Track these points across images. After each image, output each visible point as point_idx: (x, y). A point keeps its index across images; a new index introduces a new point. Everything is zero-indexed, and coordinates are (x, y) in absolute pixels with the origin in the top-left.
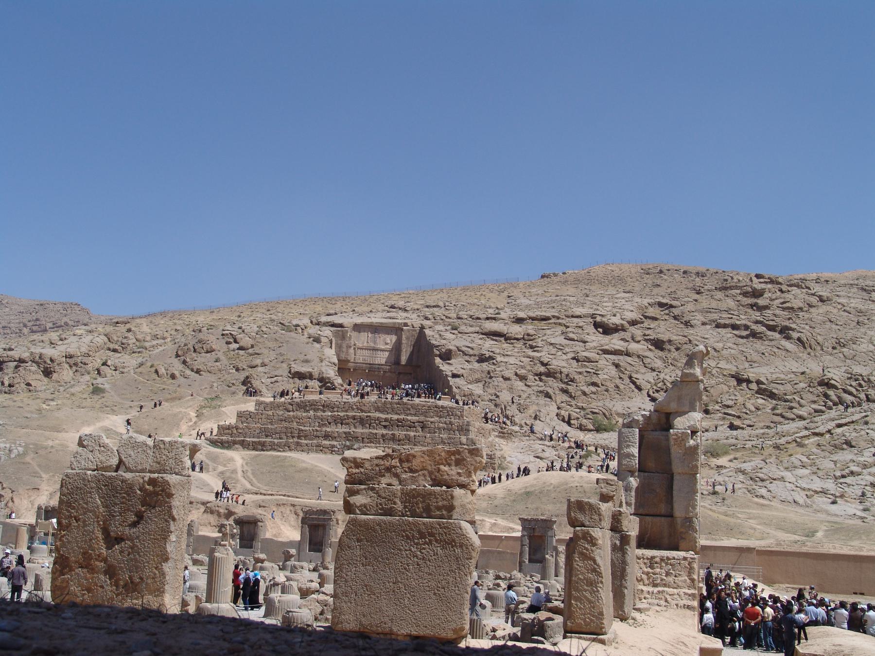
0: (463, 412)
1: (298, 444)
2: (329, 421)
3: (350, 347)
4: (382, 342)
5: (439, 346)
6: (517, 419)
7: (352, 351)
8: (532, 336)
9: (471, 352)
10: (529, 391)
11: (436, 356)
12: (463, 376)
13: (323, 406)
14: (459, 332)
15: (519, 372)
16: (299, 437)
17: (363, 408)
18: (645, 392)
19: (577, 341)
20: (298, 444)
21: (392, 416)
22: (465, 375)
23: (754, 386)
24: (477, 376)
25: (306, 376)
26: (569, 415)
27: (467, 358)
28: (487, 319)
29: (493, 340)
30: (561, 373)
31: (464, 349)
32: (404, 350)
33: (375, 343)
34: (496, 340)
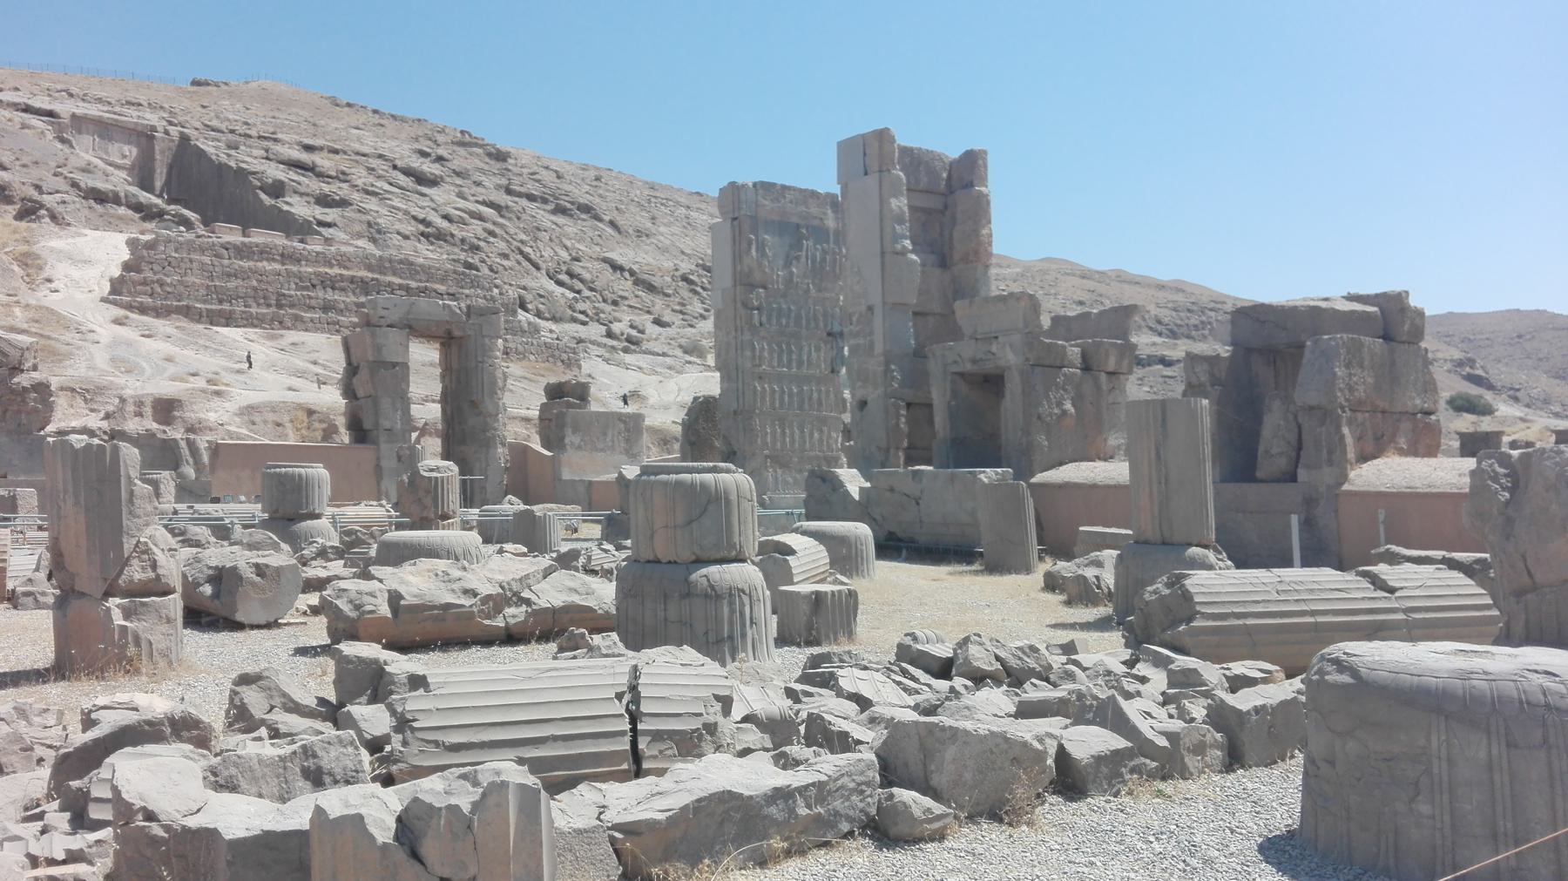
1: (297, 318)
2: (314, 282)
8: (347, 175)
12: (335, 225)
13: (282, 255)
16: (279, 306)
17: (347, 264)
18: (544, 272)
20: (297, 318)
22: (338, 223)
23: (627, 274)
24: (357, 228)
25: (107, 196)
29: (299, 174)
30: (452, 236)
32: (158, 171)
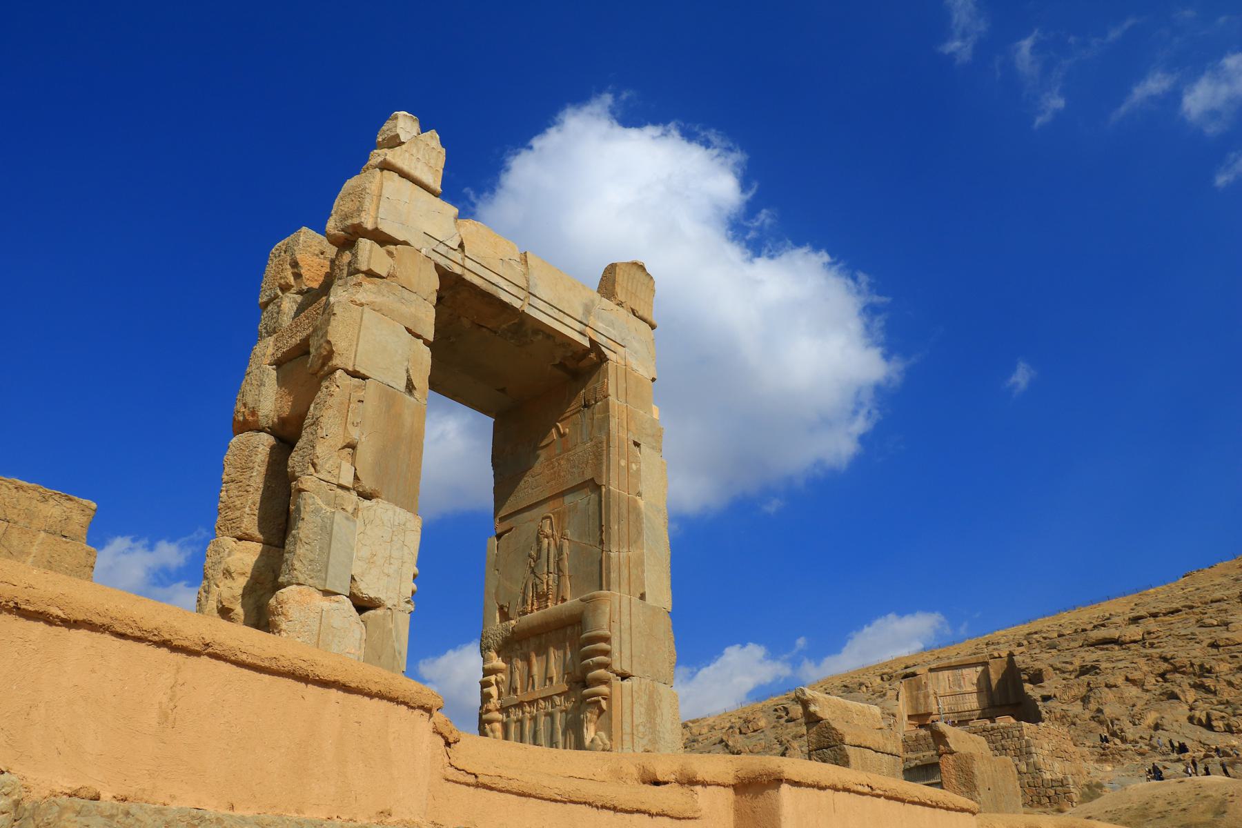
0: (1022, 730)
3: (928, 697)
4: (967, 683)
5: (1027, 668)
6: (1130, 737)
7: (932, 699)
9: (1071, 668)
10: (1147, 696)
11: (1025, 681)
12: (1055, 696)
14: (1059, 651)
15: (1130, 676)
19: (1218, 625)
21: (924, 754)
22: (1058, 695)
26: (1208, 715)
27: (1066, 676)
28: (1095, 627)
31: (1059, 666)
33: (960, 686)
34: (1107, 649)
